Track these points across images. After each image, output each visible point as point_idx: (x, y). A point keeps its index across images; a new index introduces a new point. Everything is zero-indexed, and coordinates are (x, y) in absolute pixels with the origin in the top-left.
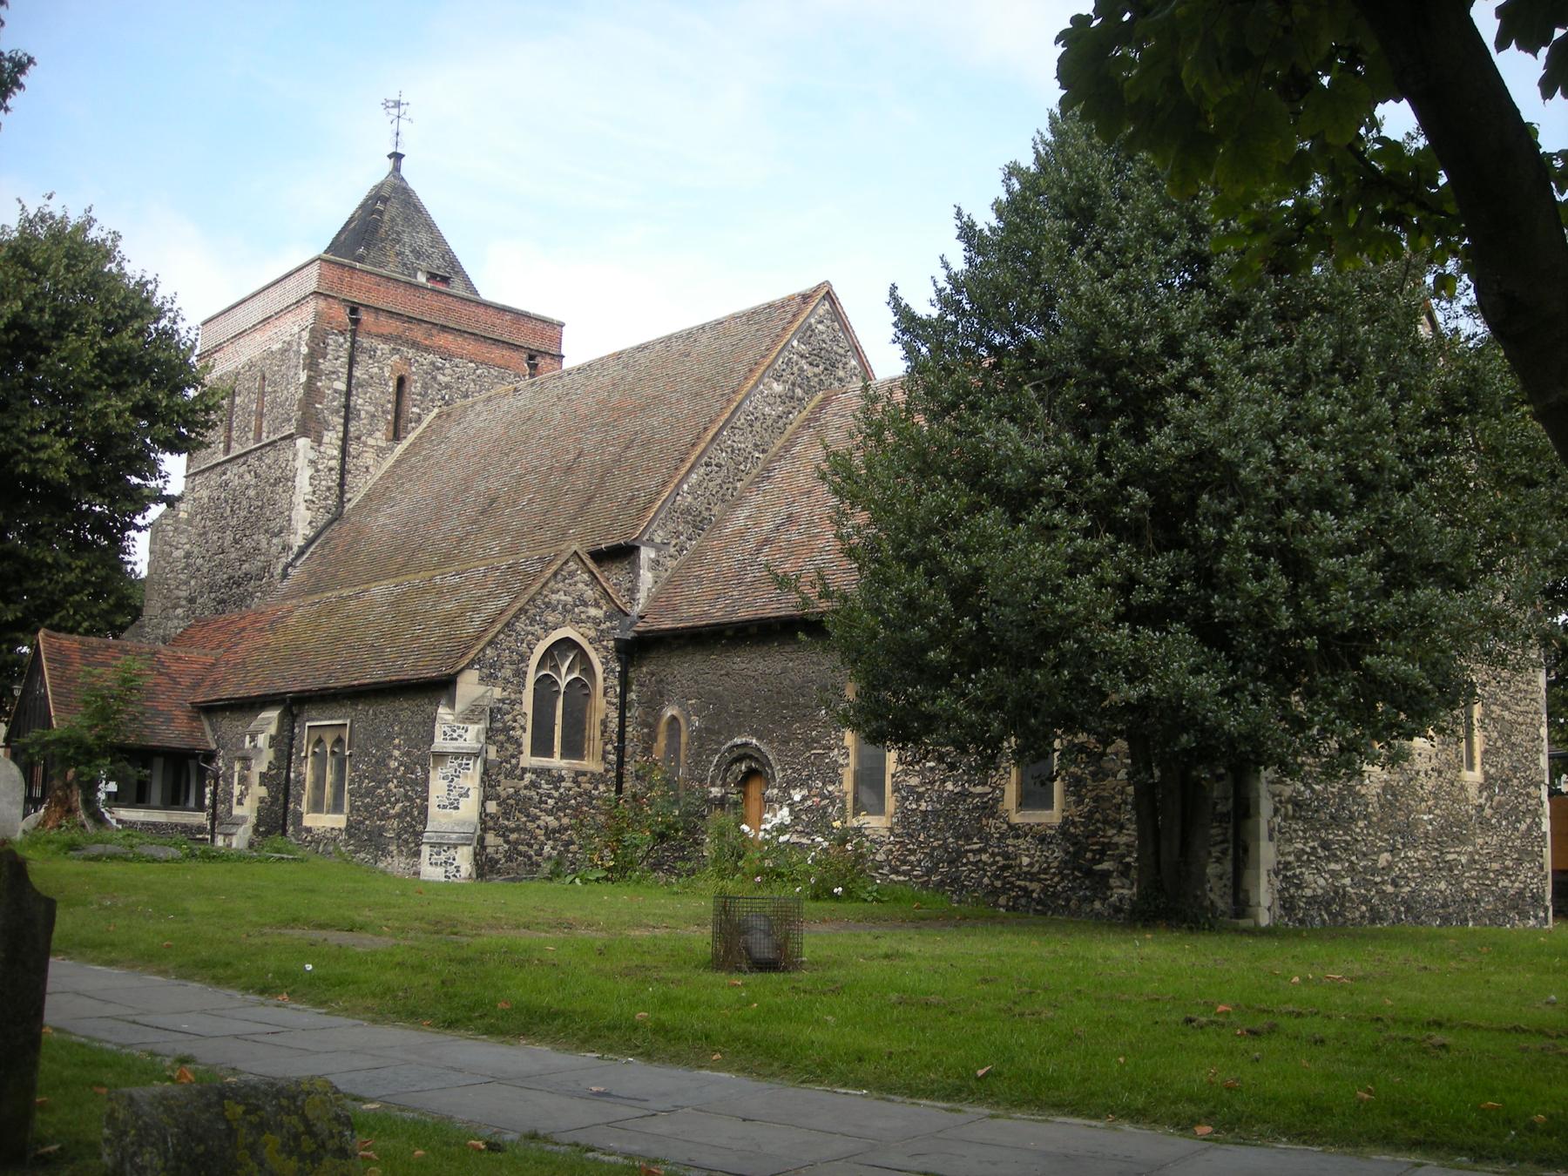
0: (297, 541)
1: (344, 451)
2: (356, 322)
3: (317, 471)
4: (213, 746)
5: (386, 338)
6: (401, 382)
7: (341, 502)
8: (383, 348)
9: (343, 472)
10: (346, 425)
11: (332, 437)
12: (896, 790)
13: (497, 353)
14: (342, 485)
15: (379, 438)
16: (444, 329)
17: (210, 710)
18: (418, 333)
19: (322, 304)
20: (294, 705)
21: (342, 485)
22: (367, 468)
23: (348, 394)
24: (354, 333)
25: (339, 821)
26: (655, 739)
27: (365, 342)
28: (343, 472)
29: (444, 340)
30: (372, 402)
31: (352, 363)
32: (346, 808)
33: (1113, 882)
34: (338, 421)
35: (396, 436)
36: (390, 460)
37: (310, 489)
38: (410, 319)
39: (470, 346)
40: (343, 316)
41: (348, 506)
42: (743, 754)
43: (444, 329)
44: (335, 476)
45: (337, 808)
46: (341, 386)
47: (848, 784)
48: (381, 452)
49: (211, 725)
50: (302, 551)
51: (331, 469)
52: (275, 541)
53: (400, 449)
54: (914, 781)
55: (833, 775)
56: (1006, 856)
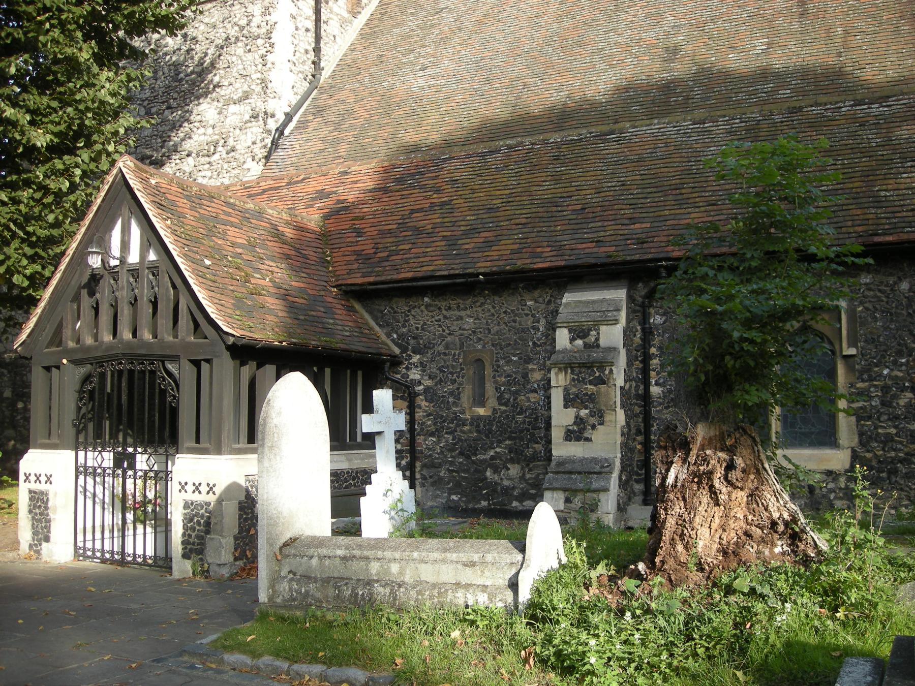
0: (280, 108)
3: (297, 29)
4: (397, 351)
9: (318, 38)
14: (317, 50)
21: (317, 50)
22: (334, 36)
28: (318, 38)
37: (292, 49)
41: (325, 74)
44: (311, 36)
45: (828, 438)
48: (343, 23)
49: (375, 319)
51: (307, 30)
52: (233, 108)
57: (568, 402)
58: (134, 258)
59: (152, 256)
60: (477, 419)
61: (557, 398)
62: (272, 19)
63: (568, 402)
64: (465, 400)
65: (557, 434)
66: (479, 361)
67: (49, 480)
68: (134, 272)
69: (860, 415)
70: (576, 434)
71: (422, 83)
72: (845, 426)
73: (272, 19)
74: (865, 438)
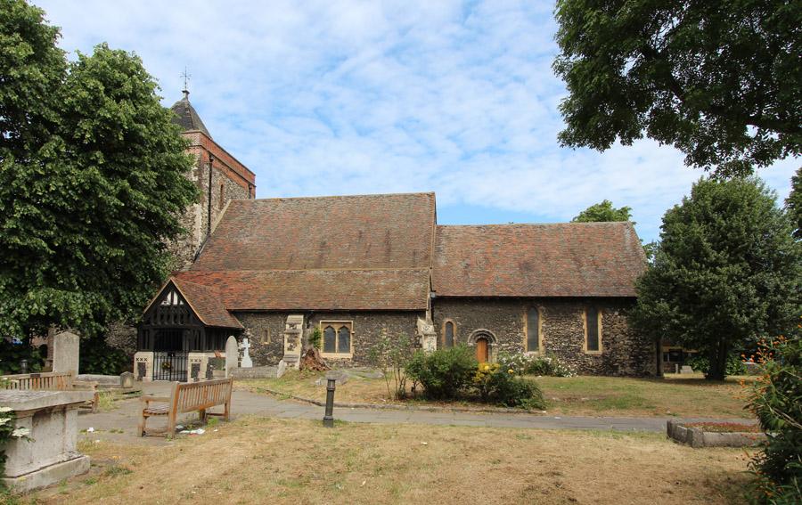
0: (198, 244)
1: (209, 211)
2: (211, 160)
5: (219, 170)
6: (222, 186)
7: (209, 229)
8: (218, 173)
10: (210, 201)
11: (206, 205)
12: (544, 345)
13: (243, 182)
14: (209, 224)
15: (216, 208)
16: (231, 170)
17: (233, 313)
18: (225, 169)
19: (203, 151)
20: (311, 315)
23: (210, 189)
24: (211, 165)
25: (349, 356)
26: (441, 328)
27: (214, 170)
29: (231, 174)
30: (215, 192)
31: (211, 177)
32: (352, 348)
33: (620, 368)
34: (207, 198)
35: (221, 209)
36: (220, 217)
38: (223, 164)
39: (237, 178)
40: (207, 156)
41: (212, 231)
42: (481, 333)
43: (231, 170)
44: (207, 219)
46: (207, 185)
47: (525, 342)
50: (201, 247)
53: (223, 212)
54: (550, 343)
55: (520, 339)
56: (584, 362)
57: (289, 341)
58: (175, 302)
59: (181, 303)
60: (265, 345)
61: (286, 340)
62: (195, 213)
63: (289, 341)
64: (263, 338)
65: (285, 349)
66: (266, 331)
67: (146, 360)
68: (176, 307)
69: (355, 346)
70: (290, 349)
71: (246, 241)
72: (352, 348)
73: (195, 213)
74: (356, 351)
